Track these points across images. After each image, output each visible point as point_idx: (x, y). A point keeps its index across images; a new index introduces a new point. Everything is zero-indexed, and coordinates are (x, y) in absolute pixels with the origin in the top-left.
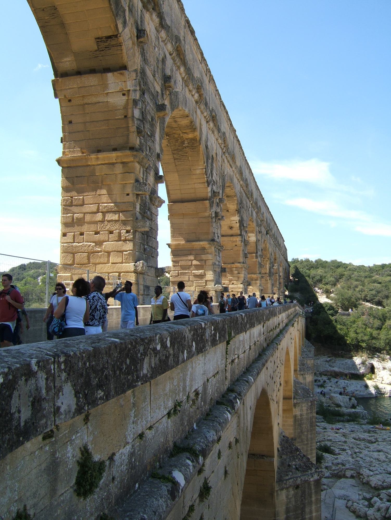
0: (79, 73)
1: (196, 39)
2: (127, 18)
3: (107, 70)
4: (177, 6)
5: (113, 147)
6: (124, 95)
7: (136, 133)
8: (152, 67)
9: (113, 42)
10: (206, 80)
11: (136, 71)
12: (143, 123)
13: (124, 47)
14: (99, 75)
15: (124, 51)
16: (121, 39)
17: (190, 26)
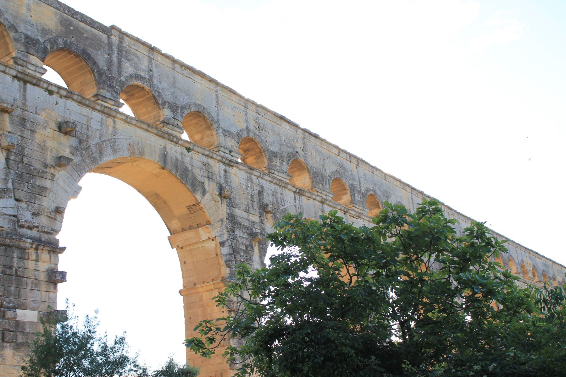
0: (183, 230)
1: (323, 140)
2: (207, 187)
3: (199, 226)
4: (288, 128)
5: (212, 278)
6: (213, 240)
7: (225, 265)
8: (244, 206)
9: (198, 207)
10: (351, 166)
11: (222, 220)
12: (234, 255)
13: (205, 209)
14: (194, 230)
15: (206, 212)
16: (202, 205)
17: (311, 134)
